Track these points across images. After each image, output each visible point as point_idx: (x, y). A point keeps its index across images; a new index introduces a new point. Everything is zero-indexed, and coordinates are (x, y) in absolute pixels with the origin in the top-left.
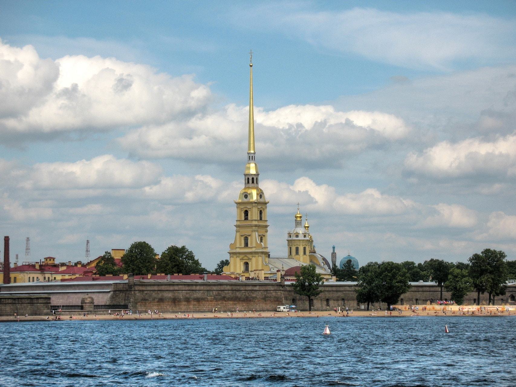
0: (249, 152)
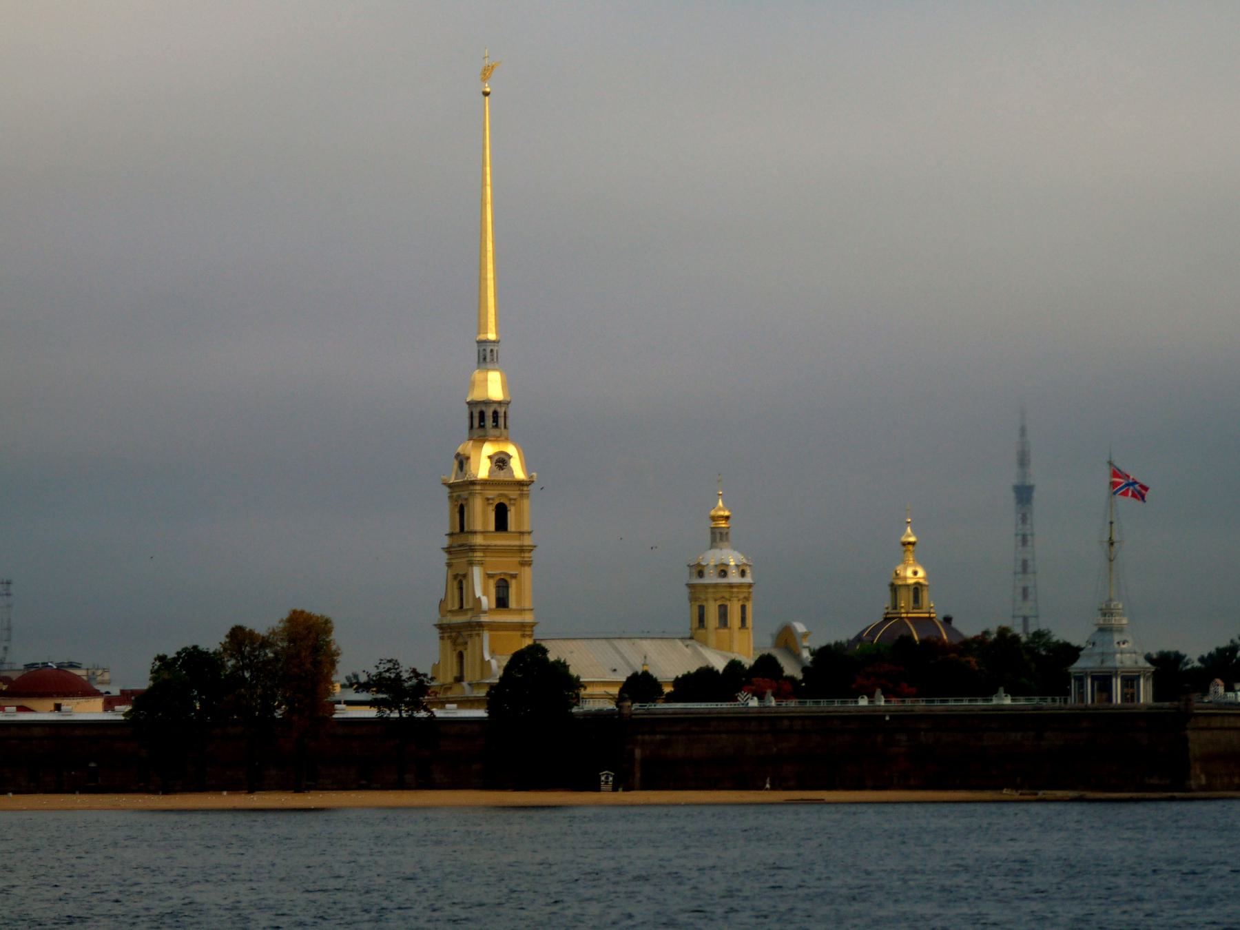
0: (482, 337)
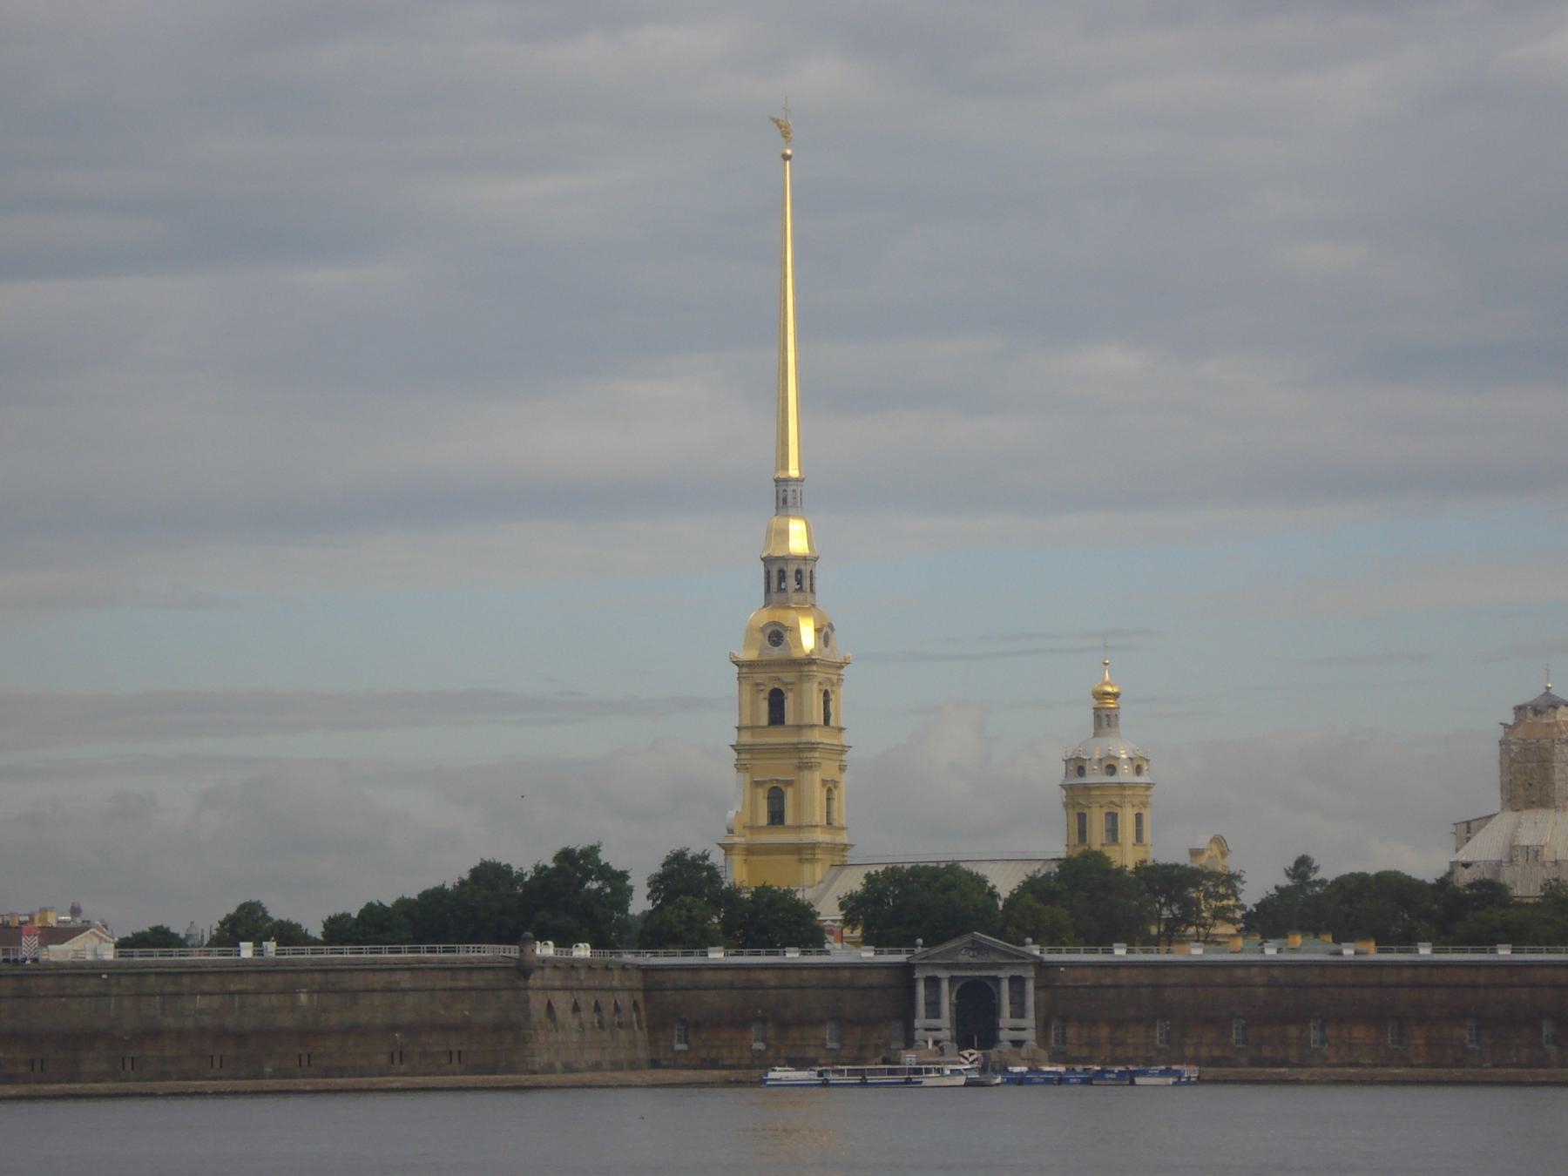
0: (781, 475)
